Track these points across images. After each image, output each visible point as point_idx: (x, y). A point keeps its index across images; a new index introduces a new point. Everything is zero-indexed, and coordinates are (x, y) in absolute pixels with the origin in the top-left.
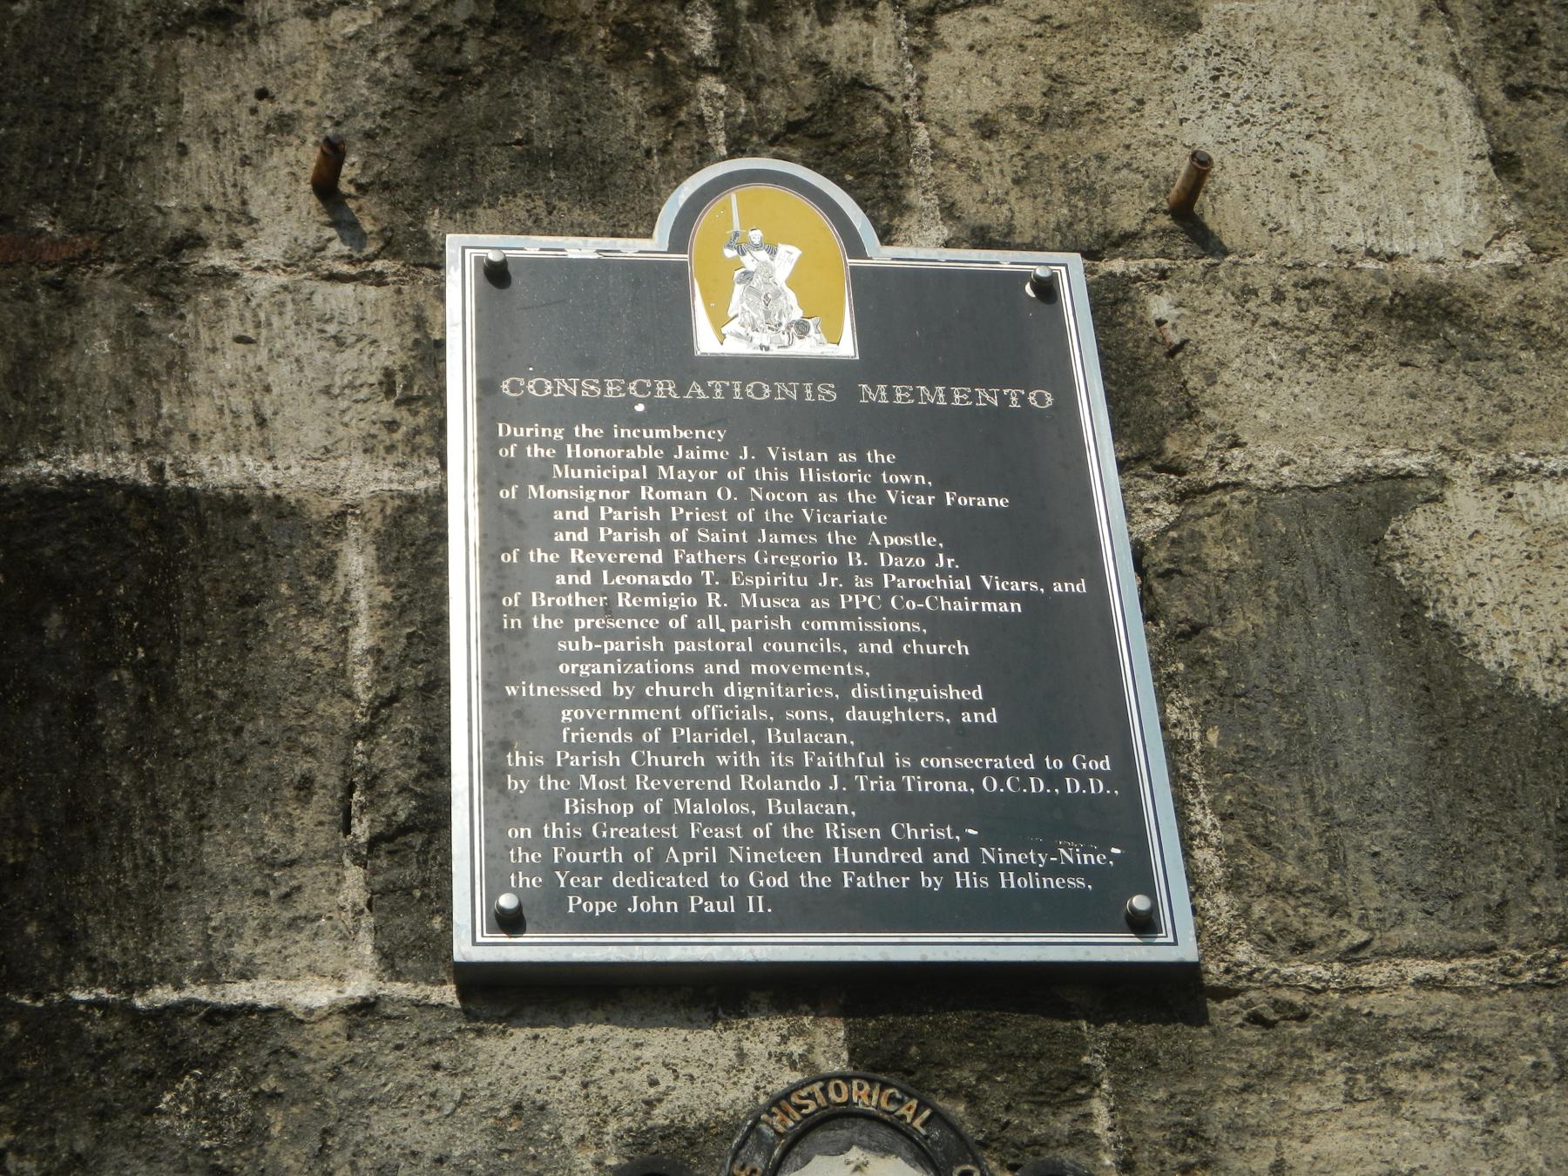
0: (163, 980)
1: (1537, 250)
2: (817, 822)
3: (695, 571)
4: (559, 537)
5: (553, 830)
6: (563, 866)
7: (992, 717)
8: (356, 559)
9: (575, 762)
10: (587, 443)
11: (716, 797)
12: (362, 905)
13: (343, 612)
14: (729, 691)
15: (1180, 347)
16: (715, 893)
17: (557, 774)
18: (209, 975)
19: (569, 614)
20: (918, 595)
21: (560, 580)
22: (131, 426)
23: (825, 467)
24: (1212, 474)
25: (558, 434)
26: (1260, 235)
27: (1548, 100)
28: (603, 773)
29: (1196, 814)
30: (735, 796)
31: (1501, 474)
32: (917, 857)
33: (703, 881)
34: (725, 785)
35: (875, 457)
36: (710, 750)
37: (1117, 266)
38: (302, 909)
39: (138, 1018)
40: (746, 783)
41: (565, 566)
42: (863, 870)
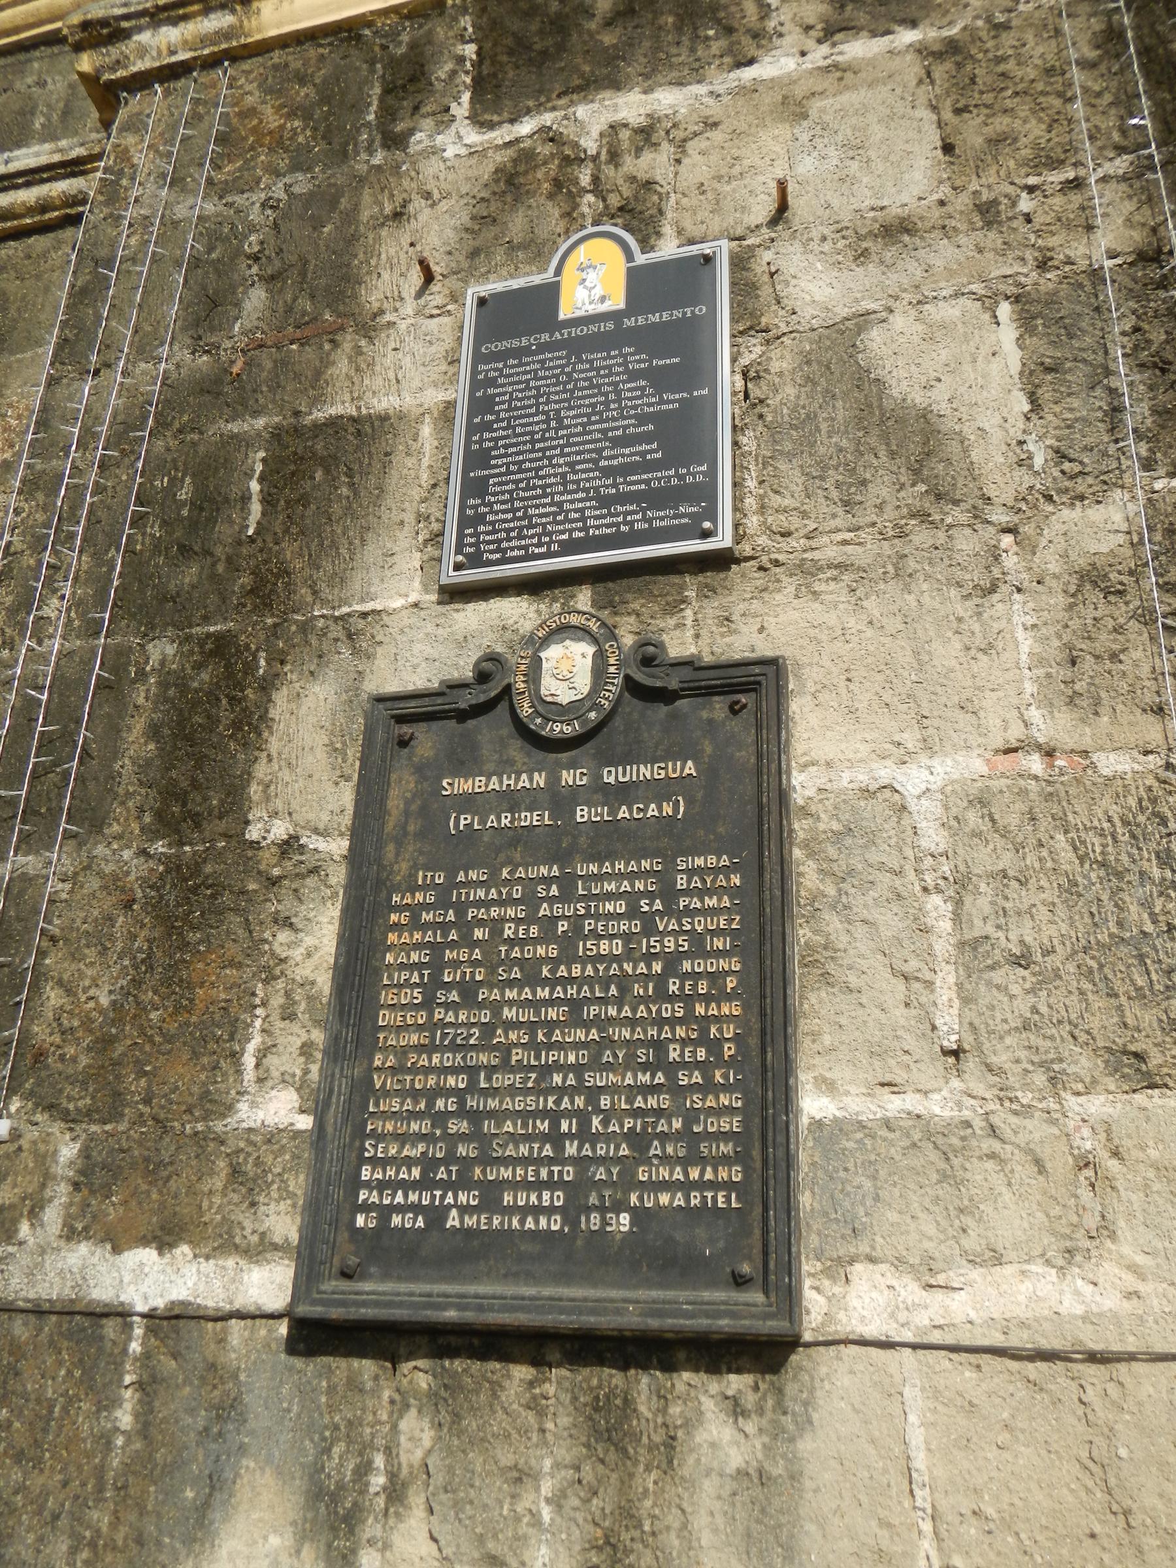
1: (955, 189)
2: (581, 510)
5: (482, 528)
6: (484, 541)
7: (659, 455)
8: (426, 430)
10: (512, 367)
11: (544, 505)
14: (554, 461)
18: (362, 600)
19: (496, 439)
20: (635, 407)
23: (605, 359)
24: (784, 328)
26: (820, 212)
27: (975, 111)
28: (503, 502)
31: (919, 302)
32: (620, 519)
34: (548, 500)
35: (627, 350)
36: (544, 487)
40: (557, 498)
41: (498, 420)
42: (597, 527)
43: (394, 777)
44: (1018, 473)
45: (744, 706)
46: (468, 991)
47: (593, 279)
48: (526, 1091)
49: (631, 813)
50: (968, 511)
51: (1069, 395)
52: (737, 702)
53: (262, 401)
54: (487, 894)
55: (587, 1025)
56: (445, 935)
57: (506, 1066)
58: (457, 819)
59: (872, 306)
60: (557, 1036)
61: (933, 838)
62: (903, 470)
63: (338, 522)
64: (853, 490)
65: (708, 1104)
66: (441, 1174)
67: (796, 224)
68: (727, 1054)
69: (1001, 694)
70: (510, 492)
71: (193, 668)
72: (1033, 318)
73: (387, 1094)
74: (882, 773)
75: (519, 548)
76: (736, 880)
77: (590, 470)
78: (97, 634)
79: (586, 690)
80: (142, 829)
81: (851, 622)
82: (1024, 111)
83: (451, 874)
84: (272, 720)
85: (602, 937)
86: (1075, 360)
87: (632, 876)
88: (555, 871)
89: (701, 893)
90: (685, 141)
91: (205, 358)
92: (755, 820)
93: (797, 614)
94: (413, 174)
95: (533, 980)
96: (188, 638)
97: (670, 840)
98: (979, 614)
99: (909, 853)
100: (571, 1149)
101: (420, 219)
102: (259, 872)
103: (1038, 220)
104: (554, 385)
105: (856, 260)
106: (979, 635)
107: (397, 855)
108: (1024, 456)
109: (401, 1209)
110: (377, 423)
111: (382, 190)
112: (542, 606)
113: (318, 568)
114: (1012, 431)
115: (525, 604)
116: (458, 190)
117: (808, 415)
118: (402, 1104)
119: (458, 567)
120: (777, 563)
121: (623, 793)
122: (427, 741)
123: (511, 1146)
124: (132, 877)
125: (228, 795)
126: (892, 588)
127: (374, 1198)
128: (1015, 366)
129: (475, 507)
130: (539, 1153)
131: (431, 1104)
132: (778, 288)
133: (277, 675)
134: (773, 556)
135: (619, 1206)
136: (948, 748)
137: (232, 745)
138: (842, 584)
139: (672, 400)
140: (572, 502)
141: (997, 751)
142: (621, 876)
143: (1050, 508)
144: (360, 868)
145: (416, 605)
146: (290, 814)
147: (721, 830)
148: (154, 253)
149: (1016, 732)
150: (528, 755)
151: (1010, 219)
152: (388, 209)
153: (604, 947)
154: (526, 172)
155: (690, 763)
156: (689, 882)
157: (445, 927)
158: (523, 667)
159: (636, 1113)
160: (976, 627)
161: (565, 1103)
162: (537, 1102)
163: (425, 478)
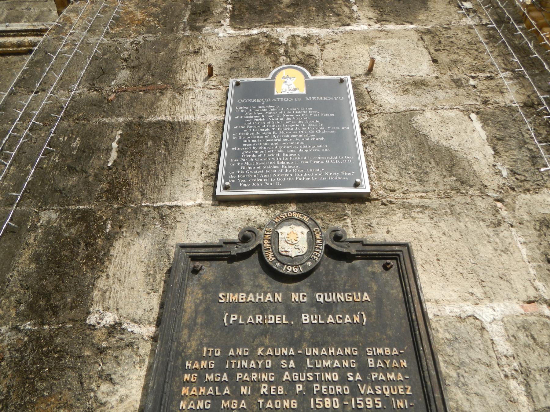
0: (160, 201)
1: (442, 74)
2: (292, 169)
3: (271, 128)
4: (245, 124)
6: (240, 178)
7: (329, 150)
8: (208, 130)
9: (244, 160)
11: (272, 165)
13: (204, 140)
15: (370, 91)
16: (270, 182)
17: (241, 163)
18: (170, 200)
19: (246, 136)
20: (315, 130)
21: (245, 131)
22: (170, 112)
23: (298, 111)
24: (376, 111)
25: (247, 108)
26: (386, 74)
29: (371, 167)
30: (276, 165)
31: (435, 109)
32: (312, 174)
34: (274, 163)
36: (271, 158)
37: (358, 79)
38: (189, 189)
39: (154, 208)
41: (246, 129)
42: (300, 177)
43: (189, 290)
44: (497, 177)
45: (391, 267)
47: (290, 82)
49: (335, 319)
50: (478, 190)
51: (511, 149)
52: (389, 264)
53: (122, 111)
54: (249, 364)
56: (221, 391)
58: (229, 317)
59: (415, 108)
61: (504, 347)
62: (444, 170)
63: (159, 164)
64: (422, 175)
67: (377, 76)
69: (519, 273)
70: (254, 158)
71: (66, 226)
72: (487, 120)
74: (468, 308)
75: (259, 182)
76: (404, 364)
77: (294, 153)
78: (12, 205)
79: (305, 250)
80: (17, 314)
81: (434, 233)
82: (463, 53)
83: (225, 351)
84: (112, 256)
86: (510, 137)
87: (340, 358)
88: (292, 352)
89: (385, 370)
90: (324, 44)
91: (95, 93)
92: (408, 328)
93: (405, 227)
94: (204, 40)
96: (66, 211)
97: (360, 337)
98: (497, 235)
99: (493, 354)
101: (206, 54)
102: (93, 344)
103: (480, 87)
104: (274, 118)
105: (403, 92)
106: (500, 244)
107: (190, 336)
108: (497, 171)
110: (182, 125)
111: (189, 43)
112: (270, 211)
113: (146, 183)
114: (489, 160)
115: (260, 210)
116: (224, 47)
117: (395, 144)
119: (226, 188)
120: (391, 202)
121: (328, 308)
122: (209, 272)
124: (5, 343)
125: (78, 296)
128: (485, 137)
129: (235, 163)
132: (372, 97)
133: (118, 233)
134: (389, 199)
136: (499, 298)
137: (84, 268)
138: (425, 215)
139: (332, 130)
140: (286, 165)
141: (524, 302)
143: (515, 193)
144: (166, 343)
145: (200, 205)
146: (117, 309)
147: (389, 333)
148: (76, 51)
149: (532, 293)
150: (270, 283)
151: (467, 86)
152: (191, 50)
154: (255, 46)
155: (366, 294)
156: (376, 363)
157: (221, 385)
158: (268, 236)
160: (497, 240)
163: (206, 149)
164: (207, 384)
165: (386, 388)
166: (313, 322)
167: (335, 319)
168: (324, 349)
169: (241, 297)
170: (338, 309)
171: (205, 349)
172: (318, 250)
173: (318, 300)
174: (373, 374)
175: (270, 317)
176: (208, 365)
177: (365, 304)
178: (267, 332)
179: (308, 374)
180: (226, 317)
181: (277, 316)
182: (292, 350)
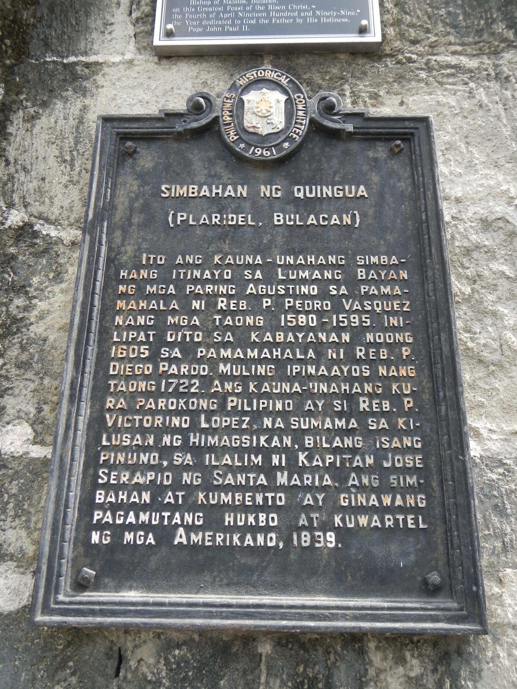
12: (132, 35)
16: (233, 25)
32: (296, 14)
33: (230, 22)
39: (65, 66)
42: (279, 18)
46: (188, 350)
48: (242, 432)
49: (318, 221)
54: (202, 274)
55: (291, 380)
57: (222, 410)
58: (175, 216)
60: (266, 387)
65: (394, 445)
66: (169, 498)
68: (407, 406)
73: (117, 430)
74: (498, 209)
75: (217, 26)
76: (404, 275)
79: (281, 126)
84: (11, 134)
85: (299, 312)
87: (321, 267)
88: (259, 260)
89: (378, 283)
95: (244, 343)
100: (282, 479)
107: (123, 240)
109: (131, 528)
118: (132, 439)
119: (169, 34)
121: (310, 205)
123: (230, 476)
126: (494, 86)
127: (108, 518)
130: (255, 481)
131: (158, 440)
133: (14, 102)
134: (408, 55)
135: (326, 526)
142: (311, 267)
146: (25, 207)
153: (302, 319)
155: (362, 188)
156: (367, 275)
157: (167, 298)
159: (336, 451)
161: (275, 442)
162: (251, 441)
164: (150, 297)
165: (378, 304)
166: (288, 223)
167: (318, 221)
168: (301, 257)
169: (192, 190)
170: (324, 207)
171: (145, 255)
172: (299, 126)
173: (296, 195)
174: (362, 287)
175: (230, 216)
176: (149, 274)
177: (361, 200)
178: (227, 236)
179: (279, 288)
180: (171, 216)
181: (240, 216)
182: (259, 257)
